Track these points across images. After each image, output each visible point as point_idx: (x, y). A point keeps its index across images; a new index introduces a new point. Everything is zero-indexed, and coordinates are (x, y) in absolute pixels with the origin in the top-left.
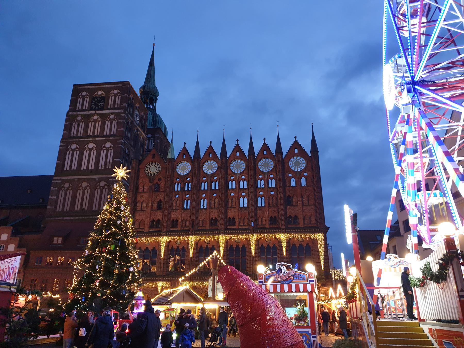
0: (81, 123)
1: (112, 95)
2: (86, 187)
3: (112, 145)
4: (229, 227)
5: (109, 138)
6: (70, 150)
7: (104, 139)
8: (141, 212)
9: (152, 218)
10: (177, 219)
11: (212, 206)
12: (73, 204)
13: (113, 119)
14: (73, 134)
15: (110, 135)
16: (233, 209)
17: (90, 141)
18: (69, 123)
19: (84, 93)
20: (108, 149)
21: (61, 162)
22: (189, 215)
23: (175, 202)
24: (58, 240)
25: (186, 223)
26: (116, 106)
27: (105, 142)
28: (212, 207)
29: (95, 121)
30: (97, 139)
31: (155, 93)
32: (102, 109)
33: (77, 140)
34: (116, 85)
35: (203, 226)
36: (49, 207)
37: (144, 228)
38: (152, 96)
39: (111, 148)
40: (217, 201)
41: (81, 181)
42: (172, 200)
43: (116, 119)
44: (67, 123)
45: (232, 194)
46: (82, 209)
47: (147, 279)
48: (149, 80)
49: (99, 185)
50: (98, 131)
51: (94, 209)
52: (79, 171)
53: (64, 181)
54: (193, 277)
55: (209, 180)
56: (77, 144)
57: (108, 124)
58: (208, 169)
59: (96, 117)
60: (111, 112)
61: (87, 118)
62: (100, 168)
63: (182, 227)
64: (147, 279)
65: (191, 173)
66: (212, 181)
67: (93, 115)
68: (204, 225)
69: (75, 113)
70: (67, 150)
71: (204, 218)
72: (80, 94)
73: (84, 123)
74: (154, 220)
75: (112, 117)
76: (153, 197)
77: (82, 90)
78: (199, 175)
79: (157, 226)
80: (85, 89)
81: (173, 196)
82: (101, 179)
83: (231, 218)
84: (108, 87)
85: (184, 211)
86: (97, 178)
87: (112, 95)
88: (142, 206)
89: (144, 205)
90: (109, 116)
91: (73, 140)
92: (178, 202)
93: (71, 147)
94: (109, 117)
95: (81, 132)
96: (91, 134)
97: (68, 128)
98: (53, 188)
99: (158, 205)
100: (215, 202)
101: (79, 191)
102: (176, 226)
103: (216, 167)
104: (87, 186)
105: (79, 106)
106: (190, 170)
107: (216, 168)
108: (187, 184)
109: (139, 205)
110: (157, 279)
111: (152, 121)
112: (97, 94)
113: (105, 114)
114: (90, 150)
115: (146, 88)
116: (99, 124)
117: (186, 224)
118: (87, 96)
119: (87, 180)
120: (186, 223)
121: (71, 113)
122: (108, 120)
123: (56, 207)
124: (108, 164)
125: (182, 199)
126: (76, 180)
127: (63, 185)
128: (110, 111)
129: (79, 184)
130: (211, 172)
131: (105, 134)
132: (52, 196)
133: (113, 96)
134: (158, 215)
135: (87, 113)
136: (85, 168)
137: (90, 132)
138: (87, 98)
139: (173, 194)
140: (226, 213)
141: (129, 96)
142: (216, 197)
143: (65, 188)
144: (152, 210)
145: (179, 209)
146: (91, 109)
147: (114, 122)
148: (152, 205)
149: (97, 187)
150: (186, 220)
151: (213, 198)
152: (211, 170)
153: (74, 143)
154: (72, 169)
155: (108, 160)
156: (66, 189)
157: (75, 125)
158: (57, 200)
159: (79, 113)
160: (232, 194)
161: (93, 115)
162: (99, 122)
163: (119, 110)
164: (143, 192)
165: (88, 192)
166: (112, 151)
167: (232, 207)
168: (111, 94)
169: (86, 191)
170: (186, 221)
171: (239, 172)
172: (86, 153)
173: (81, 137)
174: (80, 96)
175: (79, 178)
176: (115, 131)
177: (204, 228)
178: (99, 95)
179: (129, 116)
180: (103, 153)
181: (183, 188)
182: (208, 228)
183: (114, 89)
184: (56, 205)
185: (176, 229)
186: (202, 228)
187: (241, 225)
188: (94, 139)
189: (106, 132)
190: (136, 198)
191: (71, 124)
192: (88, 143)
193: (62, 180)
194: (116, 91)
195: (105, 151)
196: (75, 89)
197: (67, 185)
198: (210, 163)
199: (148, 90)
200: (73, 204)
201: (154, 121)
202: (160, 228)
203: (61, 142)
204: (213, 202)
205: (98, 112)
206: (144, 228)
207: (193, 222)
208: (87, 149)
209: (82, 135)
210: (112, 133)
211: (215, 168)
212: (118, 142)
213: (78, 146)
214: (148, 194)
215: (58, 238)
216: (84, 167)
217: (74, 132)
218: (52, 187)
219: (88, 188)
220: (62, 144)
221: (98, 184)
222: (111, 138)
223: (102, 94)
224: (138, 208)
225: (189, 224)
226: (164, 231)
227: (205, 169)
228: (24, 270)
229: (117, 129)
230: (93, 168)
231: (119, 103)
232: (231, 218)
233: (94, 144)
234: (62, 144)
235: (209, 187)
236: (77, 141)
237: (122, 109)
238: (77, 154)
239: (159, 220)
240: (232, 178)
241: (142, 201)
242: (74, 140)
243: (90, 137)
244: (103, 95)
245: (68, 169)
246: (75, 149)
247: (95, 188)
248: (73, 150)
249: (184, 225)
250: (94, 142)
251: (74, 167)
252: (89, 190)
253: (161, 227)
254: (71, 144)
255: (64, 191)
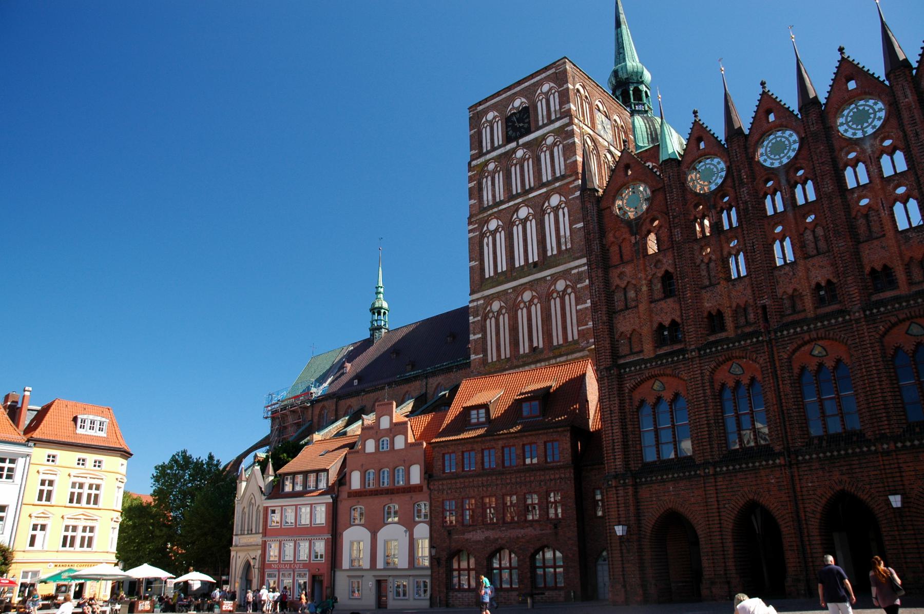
0: (497, 175)
1: (541, 98)
2: (531, 301)
3: (563, 199)
4: (874, 298)
5: (552, 187)
6: (488, 234)
7: (544, 190)
8: (627, 312)
9: (657, 319)
10: (718, 310)
11: (811, 249)
12: (515, 343)
13: (554, 144)
14: (486, 202)
15: (556, 179)
16: (876, 242)
17: (520, 203)
18: (475, 182)
19: (490, 116)
20: (556, 209)
21: (477, 263)
22: (749, 292)
23: (703, 267)
24: (478, 416)
25: (745, 314)
26: (553, 117)
27: (547, 196)
28: (811, 254)
29: (521, 162)
30: (531, 196)
31: (641, 78)
32: (528, 132)
33: (495, 210)
34: (544, 75)
35: (794, 312)
36: (474, 358)
37: (641, 351)
38: (635, 85)
39: (563, 205)
40: (822, 234)
41: (518, 290)
42: (695, 263)
43: (558, 143)
44: (472, 184)
45: (864, 202)
46: (534, 350)
47: (673, 477)
48: (621, 55)
49: (555, 291)
50: (530, 180)
51: (555, 343)
52: (512, 272)
53: (489, 299)
54: (797, 457)
55: (783, 182)
56: (497, 218)
57: (545, 158)
58: (772, 156)
59: (520, 153)
60: (545, 132)
61: (505, 160)
62: (549, 254)
63: (736, 327)
64: (673, 477)
65: (729, 180)
66: (792, 182)
67: (514, 151)
68: (799, 307)
69: (482, 160)
70: (482, 235)
71: (795, 290)
72: (484, 119)
73: (501, 173)
74: (661, 327)
75: (550, 140)
76: (648, 268)
77: (485, 112)
78: (753, 177)
79: (674, 340)
80: (488, 107)
81: (697, 253)
82: (555, 278)
83: (878, 268)
84: (530, 85)
85: (733, 285)
86: (548, 276)
87: (541, 98)
88: (626, 298)
89: (631, 294)
90: (544, 142)
91: (489, 213)
92: (712, 265)
93: (487, 227)
94: (545, 144)
95: (500, 195)
96: (519, 191)
97: (476, 192)
98: (474, 318)
99: (664, 286)
100: (815, 237)
101: (520, 311)
102: (723, 328)
103: (795, 142)
104: (533, 298)
105: (486, 145)
106: (724, 174)
107: (796, 146)
108: (724, 215)
109: (618, 296)
110: (698, 472)
111: (647, 134)
112: (513, 108)
113: (536, 139)
114: (524, 222)
115: (620, 74)
116: (529, 166)
117: (746, 318)
118: (497, 119)
119: (531, 286)
120: (745, 314)
121: (474, 163)
122: (545, 149)
123: (486, 355)
124: (563, 240)
125: (722, 255)
126: (509, 291)
127: (489, 308)
128: (543, 129)
129: (517, 297)
130: (785, 161)
131: (544, 180)
132: (474, 334)
133: (543, 98)
134: (668, 311)
135: (503, 151)
136: (522, 263)
137: (516, 187)
138: (497, 122)
139: (696, 247)
140: (857, 255)
141: (574, 86)
142: (815, 223)
143: (493, 313)
144: (652, 301)
145: (719, 283)
146: (508, 140)
147: (556, 149)
148: (651, 289)
149: (552, 296)
150: (743, 306)
151: (806, 228)
152: (782, 155)
153: (493, 219)
154: (499, 270)
155: (562, 233)
156: (496, 314)
157: (487, 183)
158: (484, 338)
159: (488, 157)
160: (864, 202)
161: (514, 151)
162: (528, 159)
163: (561, 121)
164: (623, 262)
165: (536, 310)
166: (566, 210)
167: (870, 238)
168: (539, 96)
169: (533, 308)
170: (745, 309)
171: (870, 131)
172: (517, 231)
173: (502, 202)
174: (484, 124)
175: (515, 285)
176: (563, 167)
177: (801, 316)
178: (517, 108)
179: (584, 127)
180: (549, 221)
181: (717, 226)
182: (810, 314)
183: (540, 84)
184: (485, 351)
185: (723, 335)
186: (796, 317)
187: (915, 283)
188: (525, 198)
189: (546, 176)
190: (607, 282)
191: (480, 184)
192: (516, 209)
193: (484, 298)
194: (546, 88)
195: (552, 215)
196: (473, 114)
197: (496, 306)
198: (776, 138)
199: (625, 76)
200: (515, 343)
201: (651, 132)
202: (680, 342)
203: (470, 223)
204: (811, 237)
205: (521, 141)
206: (641, 351)
207: (764, 307)
208: (517, 223)
209: (502, 198)
210: (558, 175)
211: (793, 147)
212: (572, 188)
213: (499, 221)
214: (633, 264)
215: (478, 412)
216: (519, 261)
217: (487, 197)
218: (472, 317)
219: (536, 301)
220: (471, 227)
221: (553, 288)
222: (557, 184)
223: (522, 103)
224: (619, 305)
225: (756, 314)
226: (693, 347)
227: (765, 157)
228: (428, 484)
229: (565, 161)
230: (536, 259)
231: (557, 108)
232: (878, 268)
233: (528, 206)
234: (471, 227)
235: (789, 202)
236: (495, 212)
237: (565, 117)
238: (501, 237)
239: (674, 323)
240: (852, 155)
241: (623, 286)
242: (489, 212)
243: (518, 195)
244: (524, 105)
245: (492, 274)
246: (496, 230)
247: (549, 299)
248: (494, 233)
249: (742, 321)
250: (527, 203)
251: (502, 266)
252: (539, 305)
253: (683, 340)
254: (487, 222)
255: (493, 319)
